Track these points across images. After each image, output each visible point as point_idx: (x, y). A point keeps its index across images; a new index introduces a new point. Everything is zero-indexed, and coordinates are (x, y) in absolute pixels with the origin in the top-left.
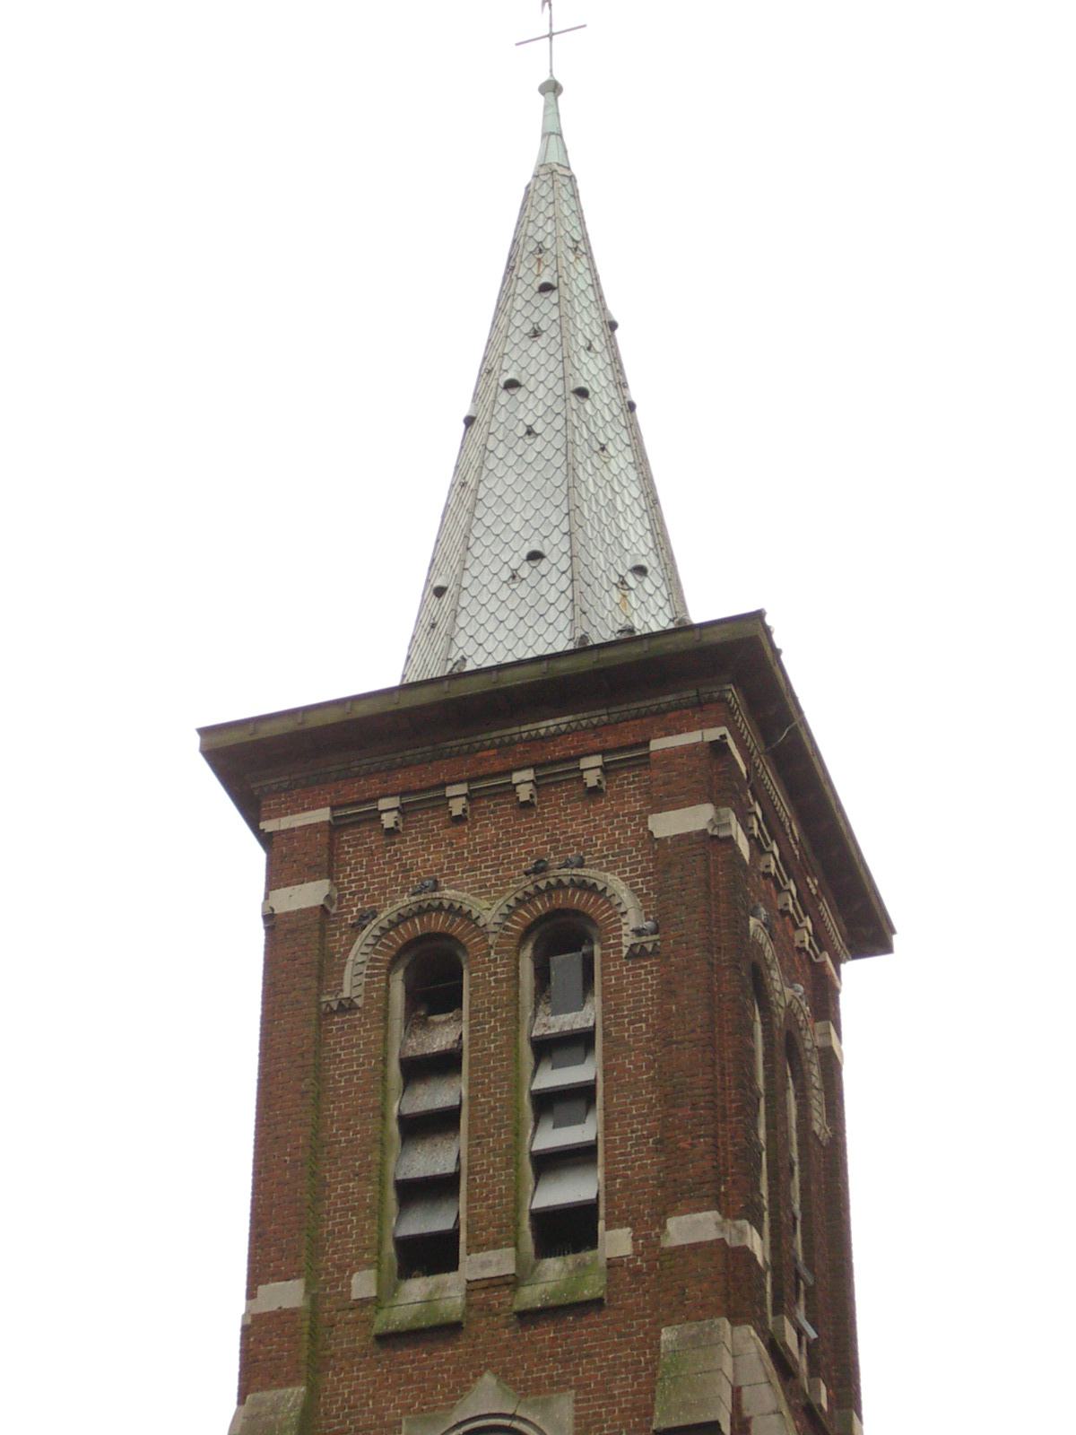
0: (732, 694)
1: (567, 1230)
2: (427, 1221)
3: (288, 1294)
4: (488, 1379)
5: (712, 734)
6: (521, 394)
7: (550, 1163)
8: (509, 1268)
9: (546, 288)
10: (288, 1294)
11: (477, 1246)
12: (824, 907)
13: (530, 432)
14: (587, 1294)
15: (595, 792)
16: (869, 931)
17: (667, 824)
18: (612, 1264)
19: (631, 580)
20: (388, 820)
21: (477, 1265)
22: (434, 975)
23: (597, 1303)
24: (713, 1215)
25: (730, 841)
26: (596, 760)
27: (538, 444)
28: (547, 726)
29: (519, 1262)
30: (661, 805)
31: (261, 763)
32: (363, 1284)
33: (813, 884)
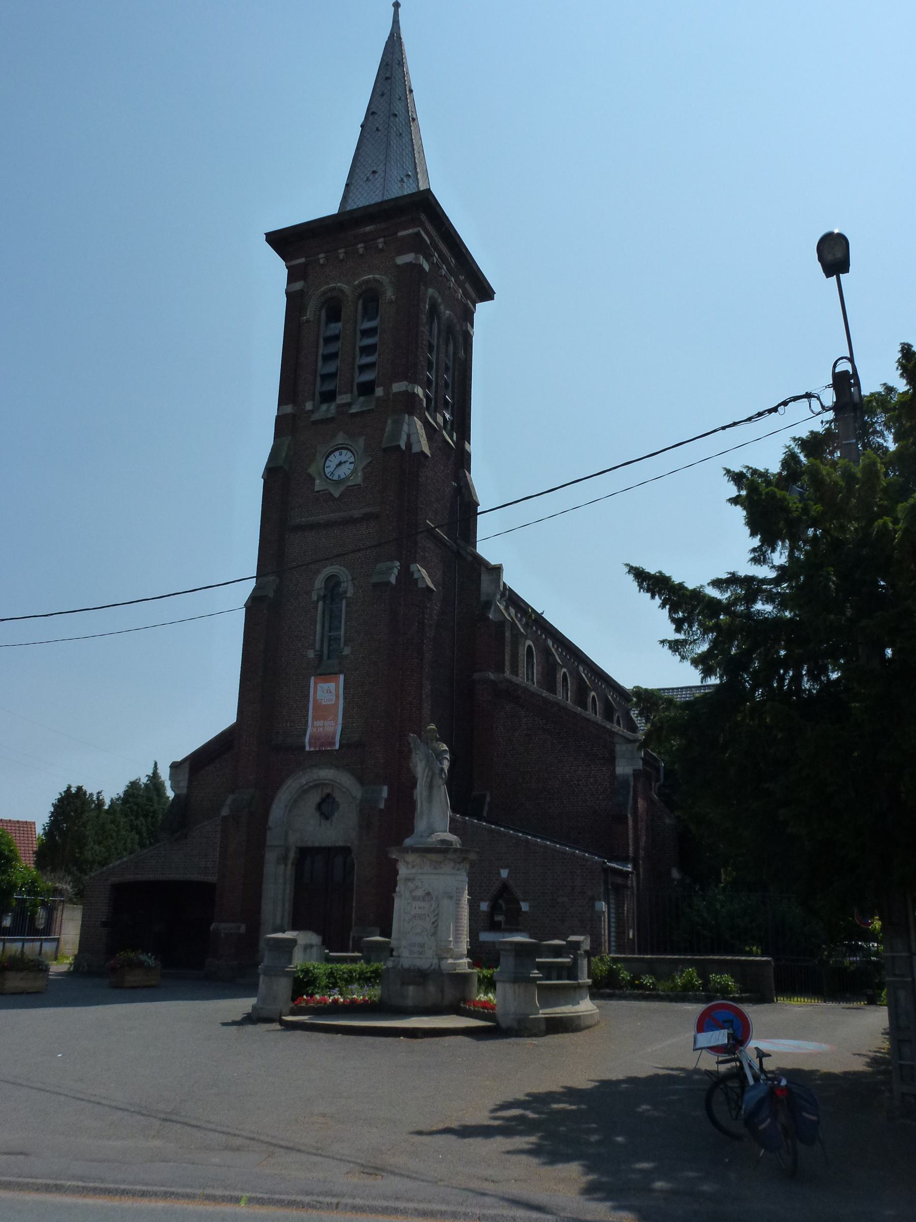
0: (423, 217)
1: (367, 389)
2: (329, 387)
3: (289, 409)
4: (341, 433)
5: (415, 230)
6: (376, 117)
7: (363, 368)
8: (349, 400)
9: (387, 78)
10: (289, 409)
11: (340, 394)
12: (467, 286)
13: (377, 129)
14: (330, 416)
15: (382, 250)
16: (486, 293)
17: (402, 260)
18: (378, 398)
19: (405, 180)
20: (322, 261)
21: (343, 399)
22: (334, 310)
23: (333, 418)
24: (405, 383)
25: (421, 266)
26: (382, 240)
27: (379, 134)
28: (368, 229)
29: (314, 406)
30: (400, 253)
31: (281, 241)
32: (309, 406)
33: (462, 278)
